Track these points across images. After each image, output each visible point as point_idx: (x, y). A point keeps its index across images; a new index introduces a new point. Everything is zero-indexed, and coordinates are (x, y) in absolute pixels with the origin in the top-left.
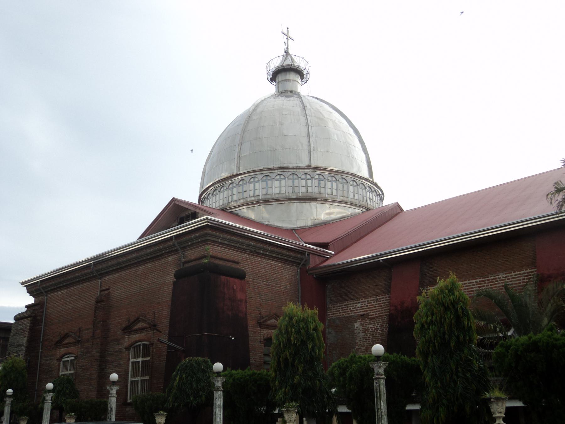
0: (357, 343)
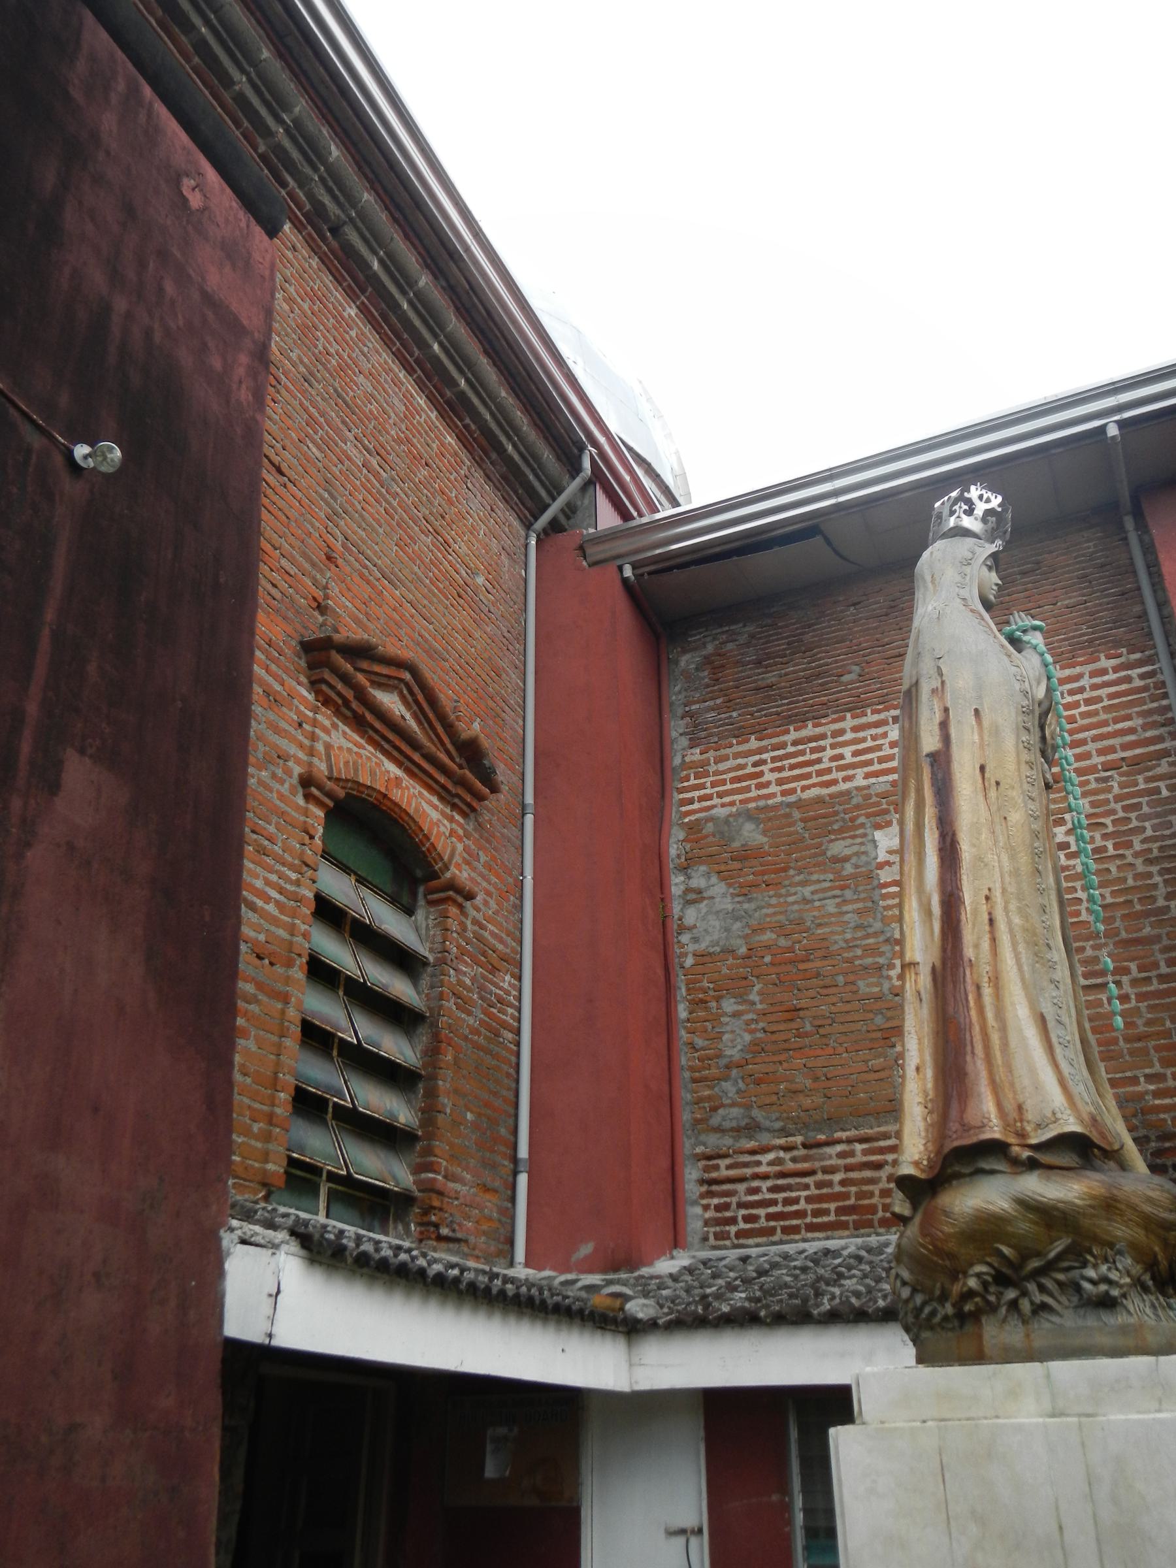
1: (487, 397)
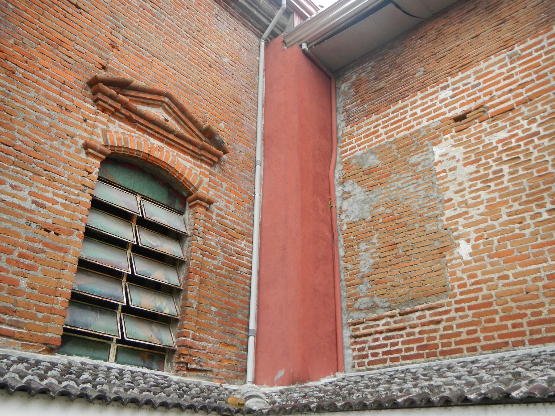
0: (450, 200)
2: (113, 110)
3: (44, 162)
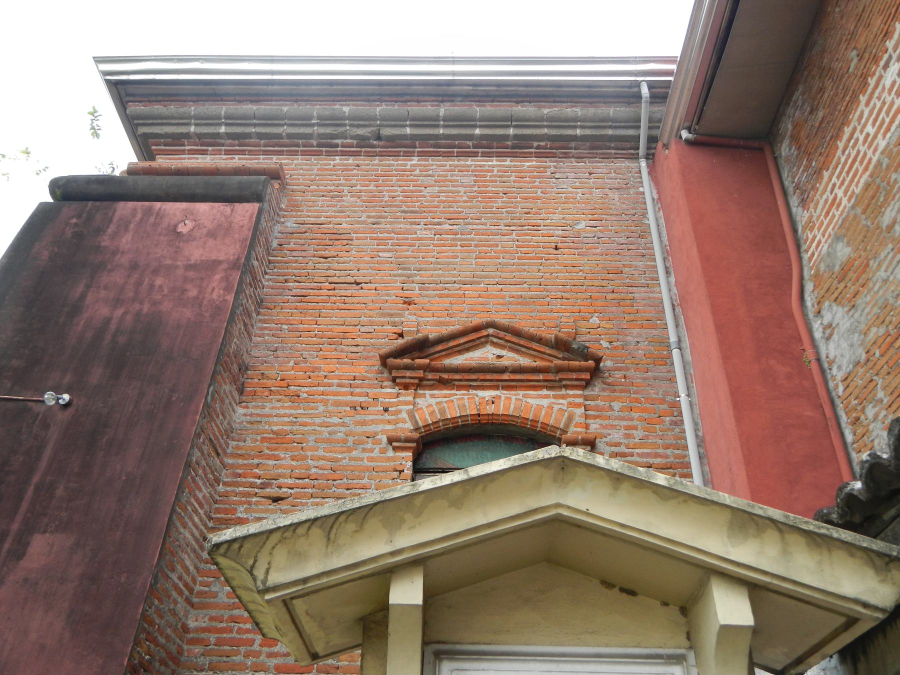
1: (538, 121)
2: (416, 381)
3: (345, 480)
